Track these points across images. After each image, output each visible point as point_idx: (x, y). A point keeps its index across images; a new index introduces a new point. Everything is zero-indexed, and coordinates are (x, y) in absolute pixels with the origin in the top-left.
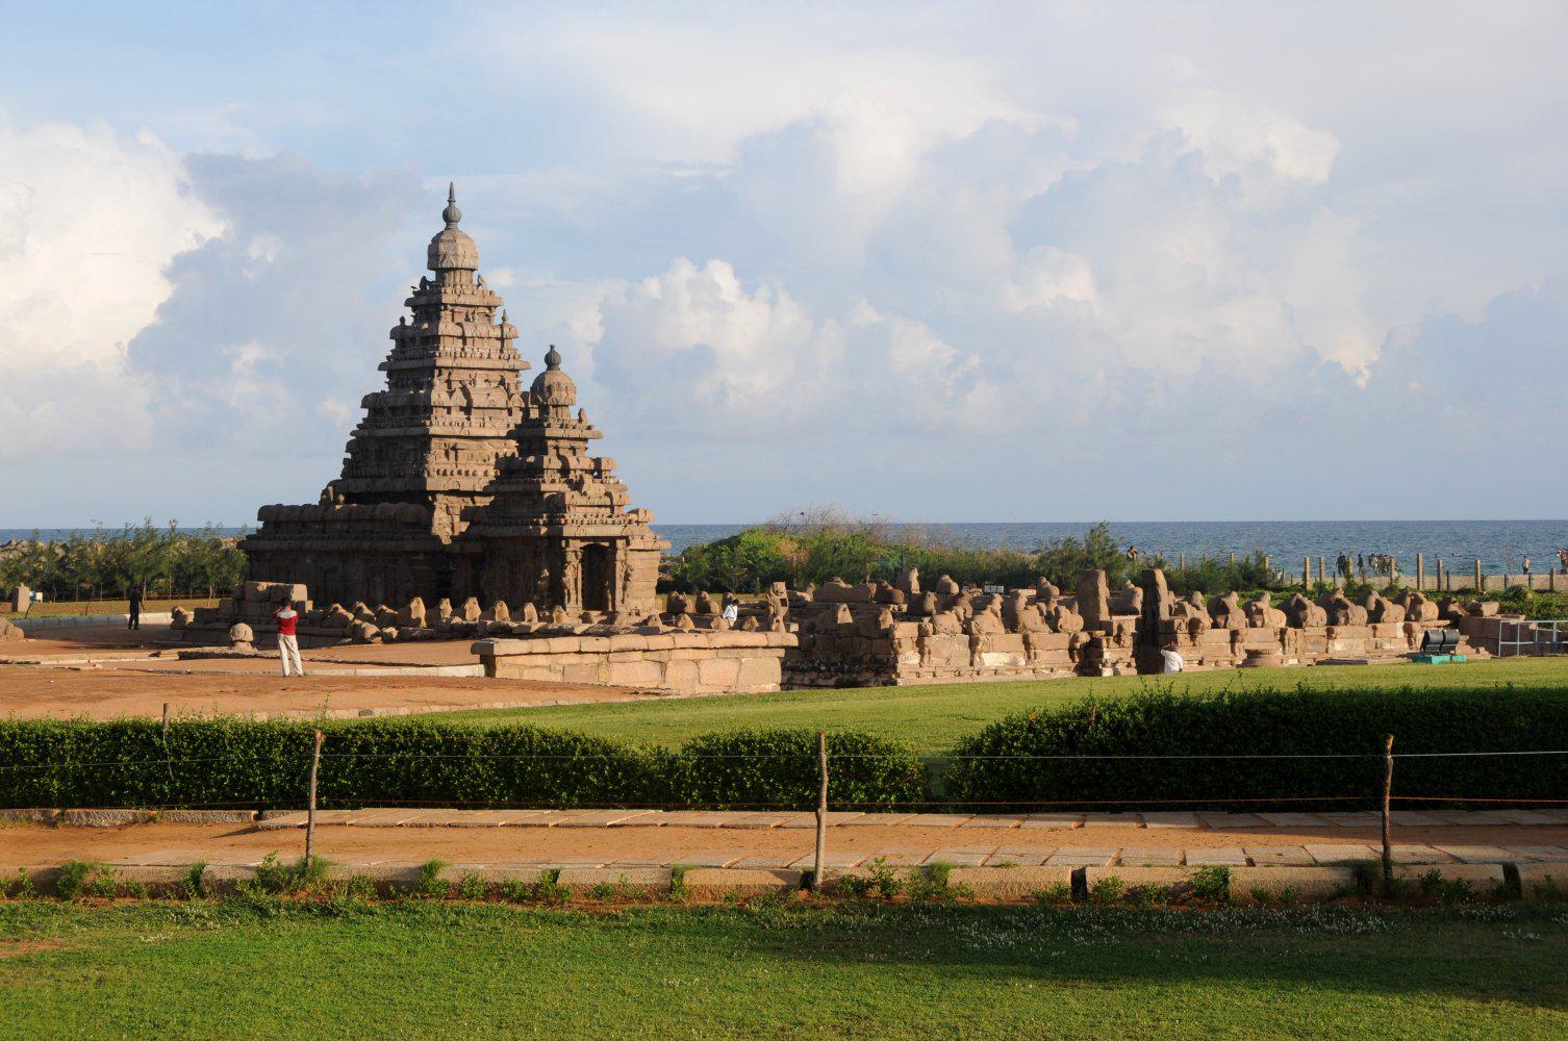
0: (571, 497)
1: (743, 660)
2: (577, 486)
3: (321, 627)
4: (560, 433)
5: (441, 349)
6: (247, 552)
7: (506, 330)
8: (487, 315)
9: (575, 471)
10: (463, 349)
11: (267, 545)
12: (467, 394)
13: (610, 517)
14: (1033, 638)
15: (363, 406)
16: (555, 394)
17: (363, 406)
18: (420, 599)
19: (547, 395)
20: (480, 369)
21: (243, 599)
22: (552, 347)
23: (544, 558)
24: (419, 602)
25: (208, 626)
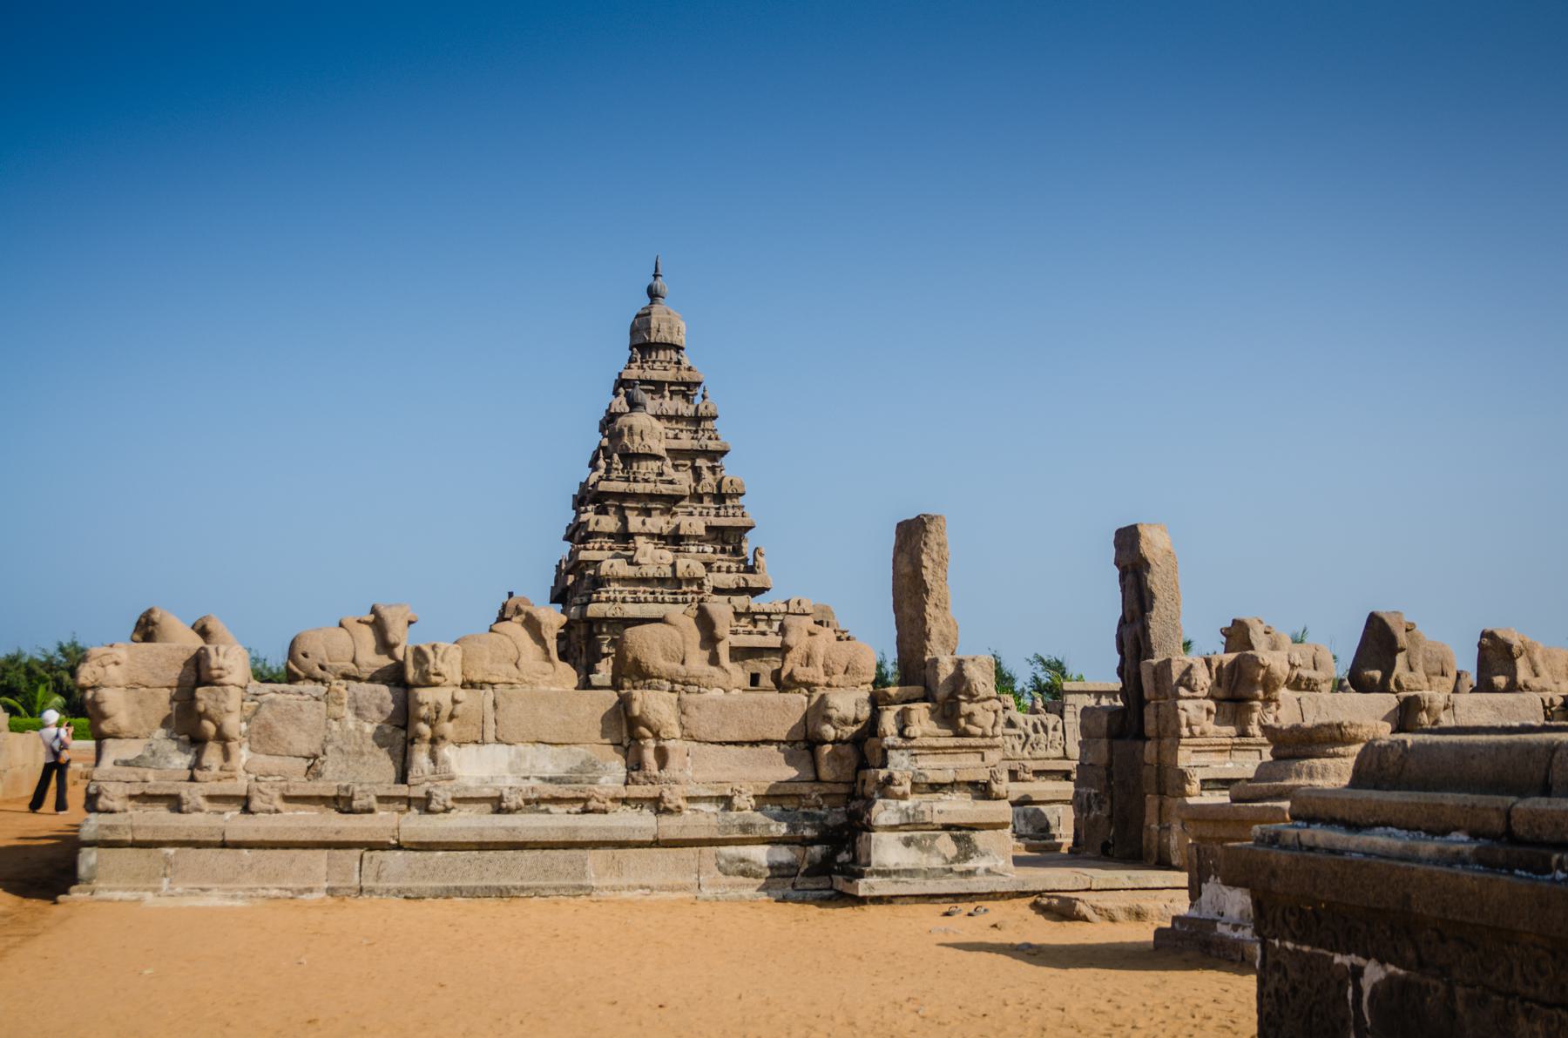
4: (620, 486)
13: (675, 593)
14: (654, 704)
16: (626, 440)
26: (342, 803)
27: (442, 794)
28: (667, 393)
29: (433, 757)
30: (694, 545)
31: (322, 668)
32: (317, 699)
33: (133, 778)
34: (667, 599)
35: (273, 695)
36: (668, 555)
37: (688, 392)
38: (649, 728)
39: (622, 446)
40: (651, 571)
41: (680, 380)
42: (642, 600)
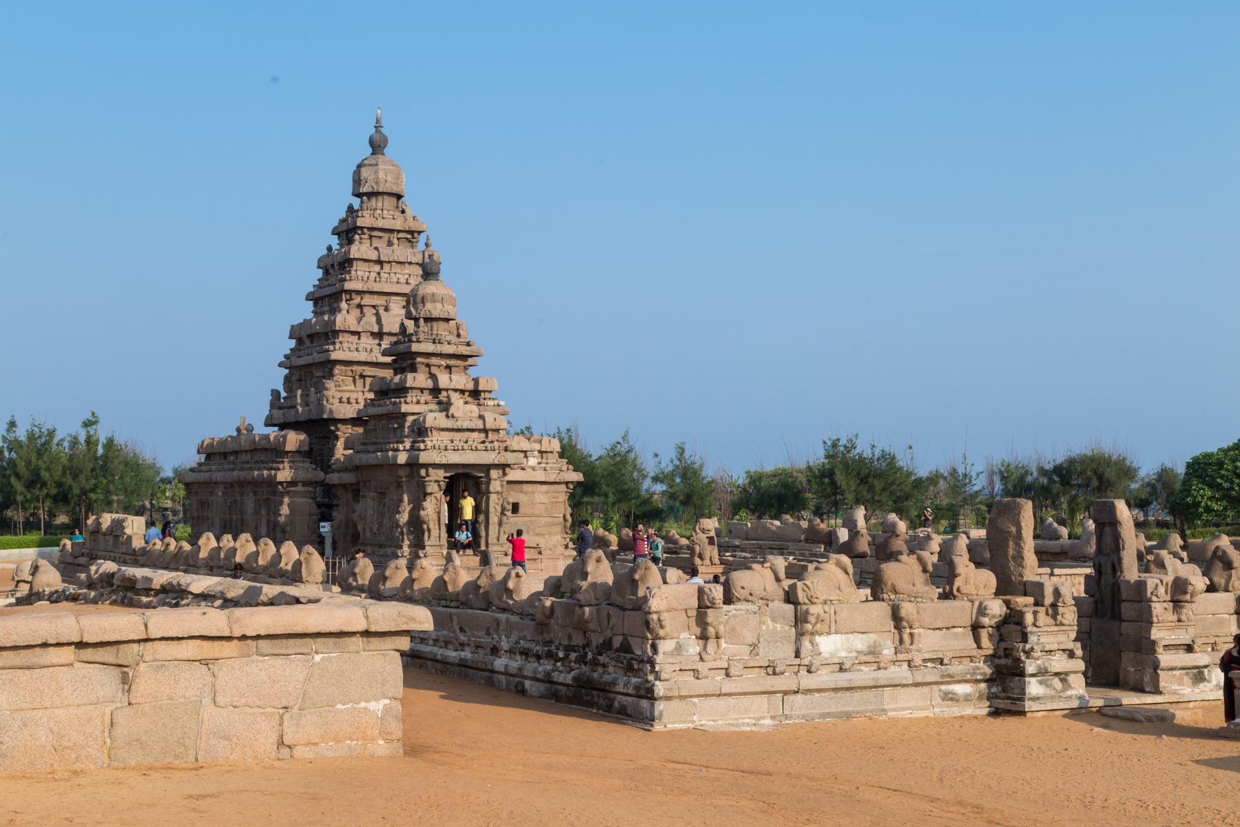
0: (434, 418)
1: (318, 658)
2: (445, 406)
4: (428, 347)
5: (353, 273)
8: (410, 241)
9: (447, 390)
10: (379, 274)
12: (379, 321)
13: (483, 442)
14: (907, 609)
15: (291, 337)
16: (429, 306)
17: (291, 337)
18: (211, 535)
19: (420, 306)
24: (208, 539)
26: (772, 670)
27: (817, 663)
29: (812, 643)
30: (490, 399)
31: (751, 595)
32: (755, 613)
33: (676, 661)
34: (479, 447)
35: (734, 612)
36: (473, 409)
37: (414, 240)
38: (908, 623)
40: (466, 425)
41: (407, 229)
42: (460, 448)
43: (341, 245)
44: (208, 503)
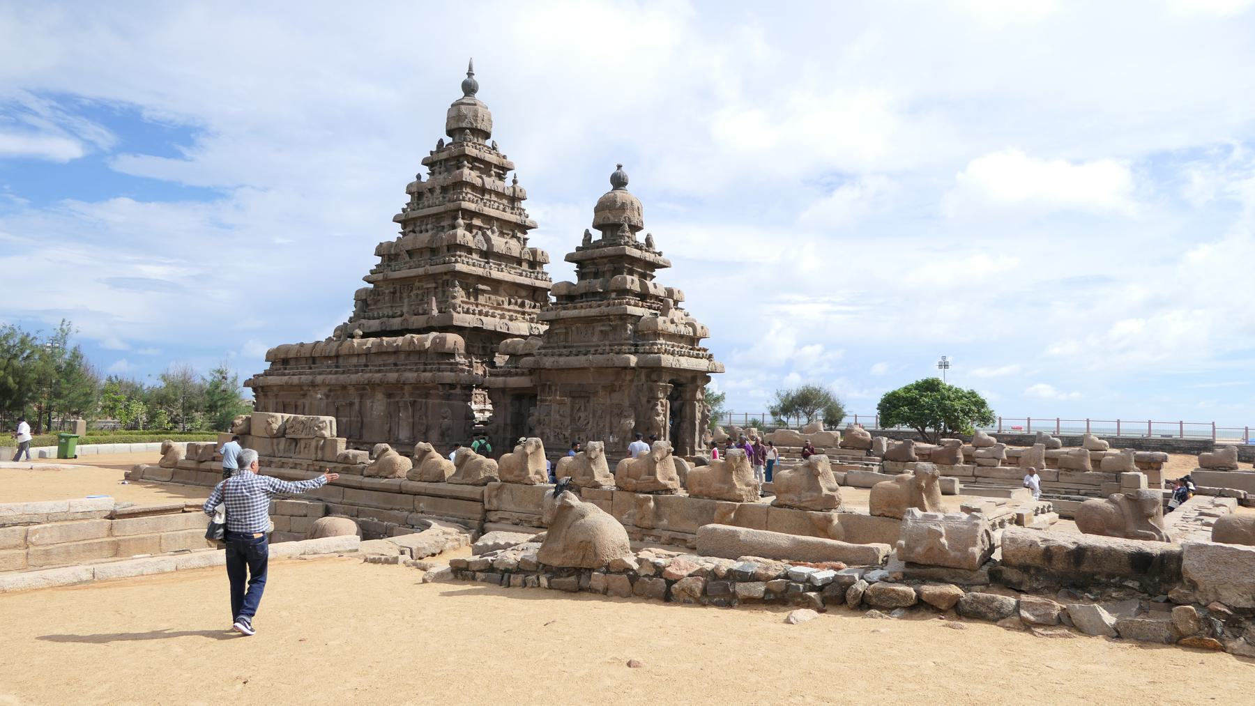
3: (362, 475)
4: (636, 253)
5: (464, 194)
6: (255, 390)
7: (518, 190)
10: (482, 199)
11: (273, 380)
12: (488, 240)
16: (628, 213)
17: (378, 253)
20: (497, 219)
21: (250, 434)
22: (619, 167)
23: (626, 392)
24: (538, 447)
25: (203, 466)
28: (493, 173)
39: (625, 217)
43: (432, 174)
44: (296, 406)
